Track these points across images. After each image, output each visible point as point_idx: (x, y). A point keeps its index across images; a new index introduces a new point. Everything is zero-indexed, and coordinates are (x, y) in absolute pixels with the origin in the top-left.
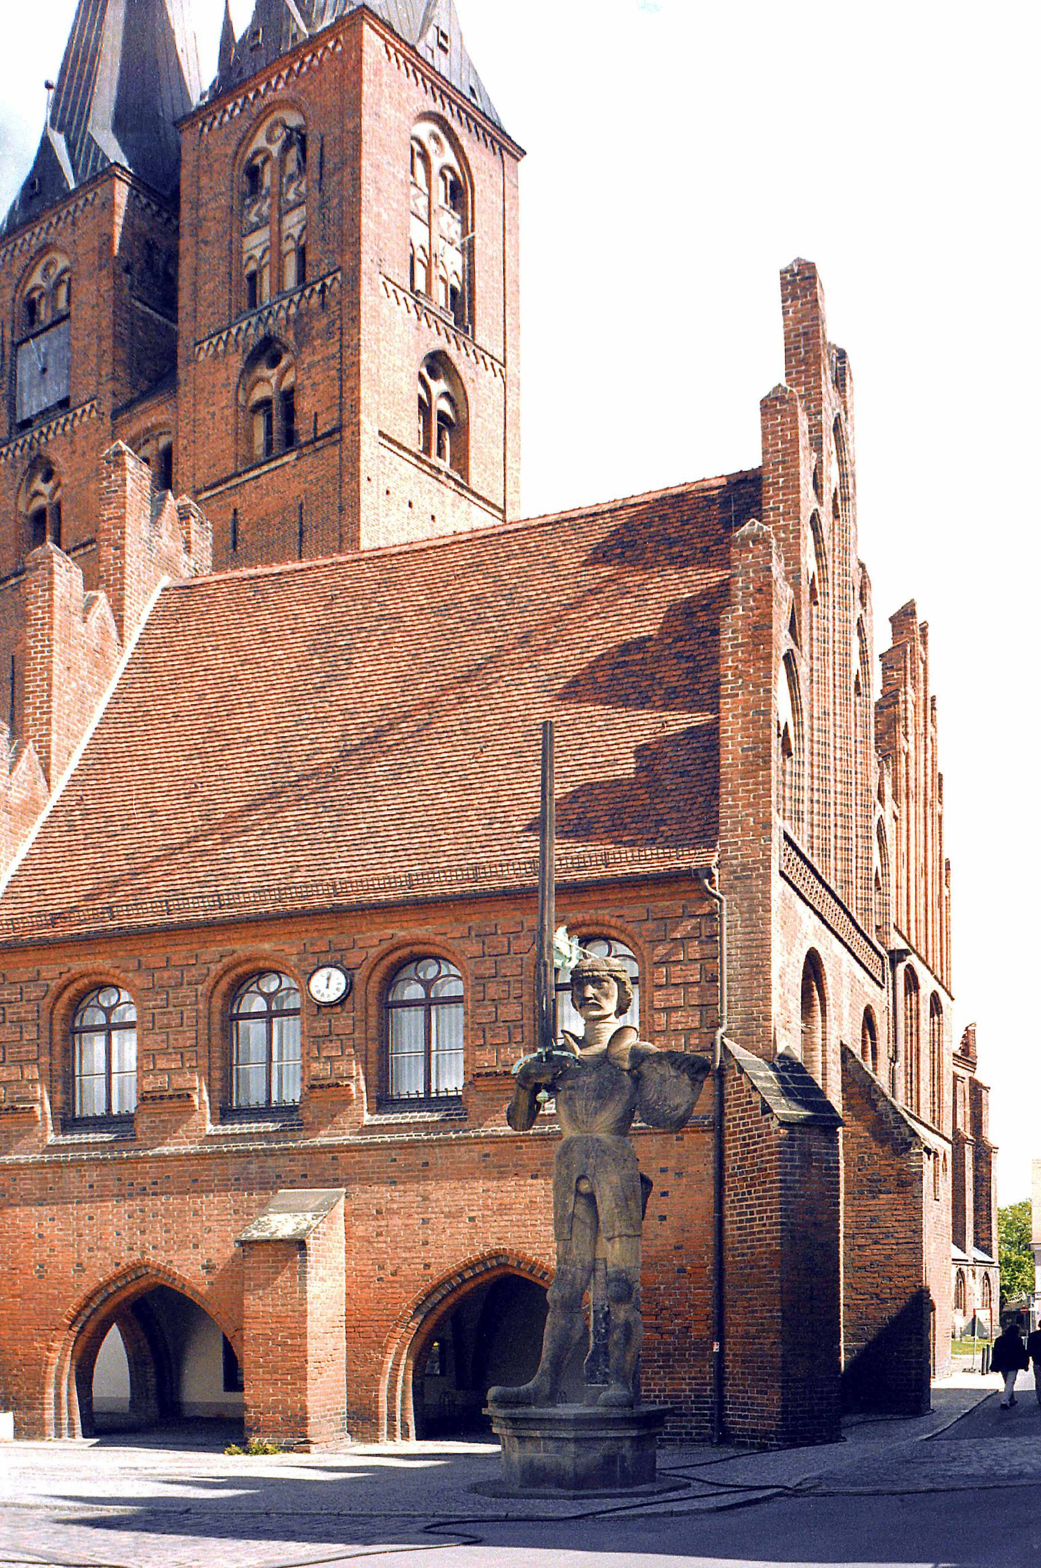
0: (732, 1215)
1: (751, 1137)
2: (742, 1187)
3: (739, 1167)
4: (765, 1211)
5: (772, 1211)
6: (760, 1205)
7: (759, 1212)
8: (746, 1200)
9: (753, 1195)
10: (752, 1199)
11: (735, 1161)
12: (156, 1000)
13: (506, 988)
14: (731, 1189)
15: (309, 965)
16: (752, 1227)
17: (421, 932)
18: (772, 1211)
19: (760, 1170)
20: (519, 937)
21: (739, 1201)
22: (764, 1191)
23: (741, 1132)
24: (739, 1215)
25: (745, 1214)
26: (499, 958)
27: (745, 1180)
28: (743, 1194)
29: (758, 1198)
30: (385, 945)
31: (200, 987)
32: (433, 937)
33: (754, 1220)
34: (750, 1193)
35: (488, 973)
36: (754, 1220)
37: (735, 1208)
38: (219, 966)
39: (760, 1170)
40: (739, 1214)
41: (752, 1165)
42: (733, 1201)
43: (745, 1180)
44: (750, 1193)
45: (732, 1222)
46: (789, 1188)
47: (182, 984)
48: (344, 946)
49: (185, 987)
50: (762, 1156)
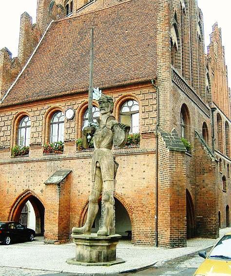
46: (172, 170)
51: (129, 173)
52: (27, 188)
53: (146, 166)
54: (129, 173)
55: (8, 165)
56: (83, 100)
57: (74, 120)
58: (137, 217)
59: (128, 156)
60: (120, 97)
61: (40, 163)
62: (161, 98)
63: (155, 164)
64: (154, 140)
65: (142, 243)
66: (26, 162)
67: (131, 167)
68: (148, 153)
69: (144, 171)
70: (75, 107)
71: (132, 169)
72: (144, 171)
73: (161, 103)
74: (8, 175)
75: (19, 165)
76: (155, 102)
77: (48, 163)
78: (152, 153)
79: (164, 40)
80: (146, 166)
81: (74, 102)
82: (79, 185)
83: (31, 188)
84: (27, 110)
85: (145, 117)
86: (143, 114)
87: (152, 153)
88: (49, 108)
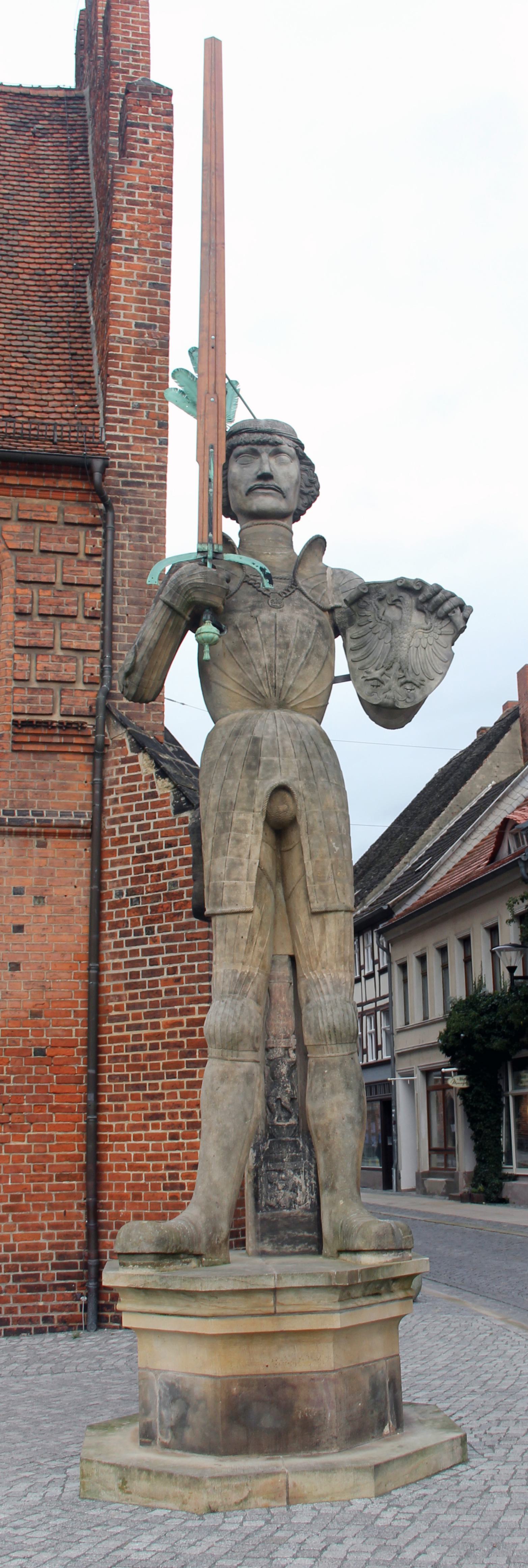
0: (116, 966)
1: (152, 847)
2: (135, 923)
3: (130, 892)
4: (180, 959)
5: (191, 959)
6: (170, 949)
7: (166, 961)
8: (144, 941)
9: (156, 934)
10: (154, 940)
11: (125, 882)
14: (114, 925)
16: (154, 984)
18: (191, 959)
19: (168, 896)
21: (129, 943)
22: (177, 927)
23: (135, 839)
24: (129, 964)
25: (142, 963)
27: (142, 911)
28: (138, 933)
29: (165, 939)
33: (160, 972)
34: (150, 931)
36: (160, 972)
37: (123, 955)
39: (168, 896)
40: (129, 964)
41: (156, 888)
42: (118, 945)
43: (142, 911)
44: (150, 931)
45: (116, 977)
50: (174, 875)
63: (80, 896)
64: (79, 768)
68: (46, 831)
69: (19, 929)
72: (19, 929)
76: (92, 573)
78: (67, 831)
79: (148, 294)
80: (28, 898)
85: (33, 641)
86: (23, 626)
87: (67, 831)
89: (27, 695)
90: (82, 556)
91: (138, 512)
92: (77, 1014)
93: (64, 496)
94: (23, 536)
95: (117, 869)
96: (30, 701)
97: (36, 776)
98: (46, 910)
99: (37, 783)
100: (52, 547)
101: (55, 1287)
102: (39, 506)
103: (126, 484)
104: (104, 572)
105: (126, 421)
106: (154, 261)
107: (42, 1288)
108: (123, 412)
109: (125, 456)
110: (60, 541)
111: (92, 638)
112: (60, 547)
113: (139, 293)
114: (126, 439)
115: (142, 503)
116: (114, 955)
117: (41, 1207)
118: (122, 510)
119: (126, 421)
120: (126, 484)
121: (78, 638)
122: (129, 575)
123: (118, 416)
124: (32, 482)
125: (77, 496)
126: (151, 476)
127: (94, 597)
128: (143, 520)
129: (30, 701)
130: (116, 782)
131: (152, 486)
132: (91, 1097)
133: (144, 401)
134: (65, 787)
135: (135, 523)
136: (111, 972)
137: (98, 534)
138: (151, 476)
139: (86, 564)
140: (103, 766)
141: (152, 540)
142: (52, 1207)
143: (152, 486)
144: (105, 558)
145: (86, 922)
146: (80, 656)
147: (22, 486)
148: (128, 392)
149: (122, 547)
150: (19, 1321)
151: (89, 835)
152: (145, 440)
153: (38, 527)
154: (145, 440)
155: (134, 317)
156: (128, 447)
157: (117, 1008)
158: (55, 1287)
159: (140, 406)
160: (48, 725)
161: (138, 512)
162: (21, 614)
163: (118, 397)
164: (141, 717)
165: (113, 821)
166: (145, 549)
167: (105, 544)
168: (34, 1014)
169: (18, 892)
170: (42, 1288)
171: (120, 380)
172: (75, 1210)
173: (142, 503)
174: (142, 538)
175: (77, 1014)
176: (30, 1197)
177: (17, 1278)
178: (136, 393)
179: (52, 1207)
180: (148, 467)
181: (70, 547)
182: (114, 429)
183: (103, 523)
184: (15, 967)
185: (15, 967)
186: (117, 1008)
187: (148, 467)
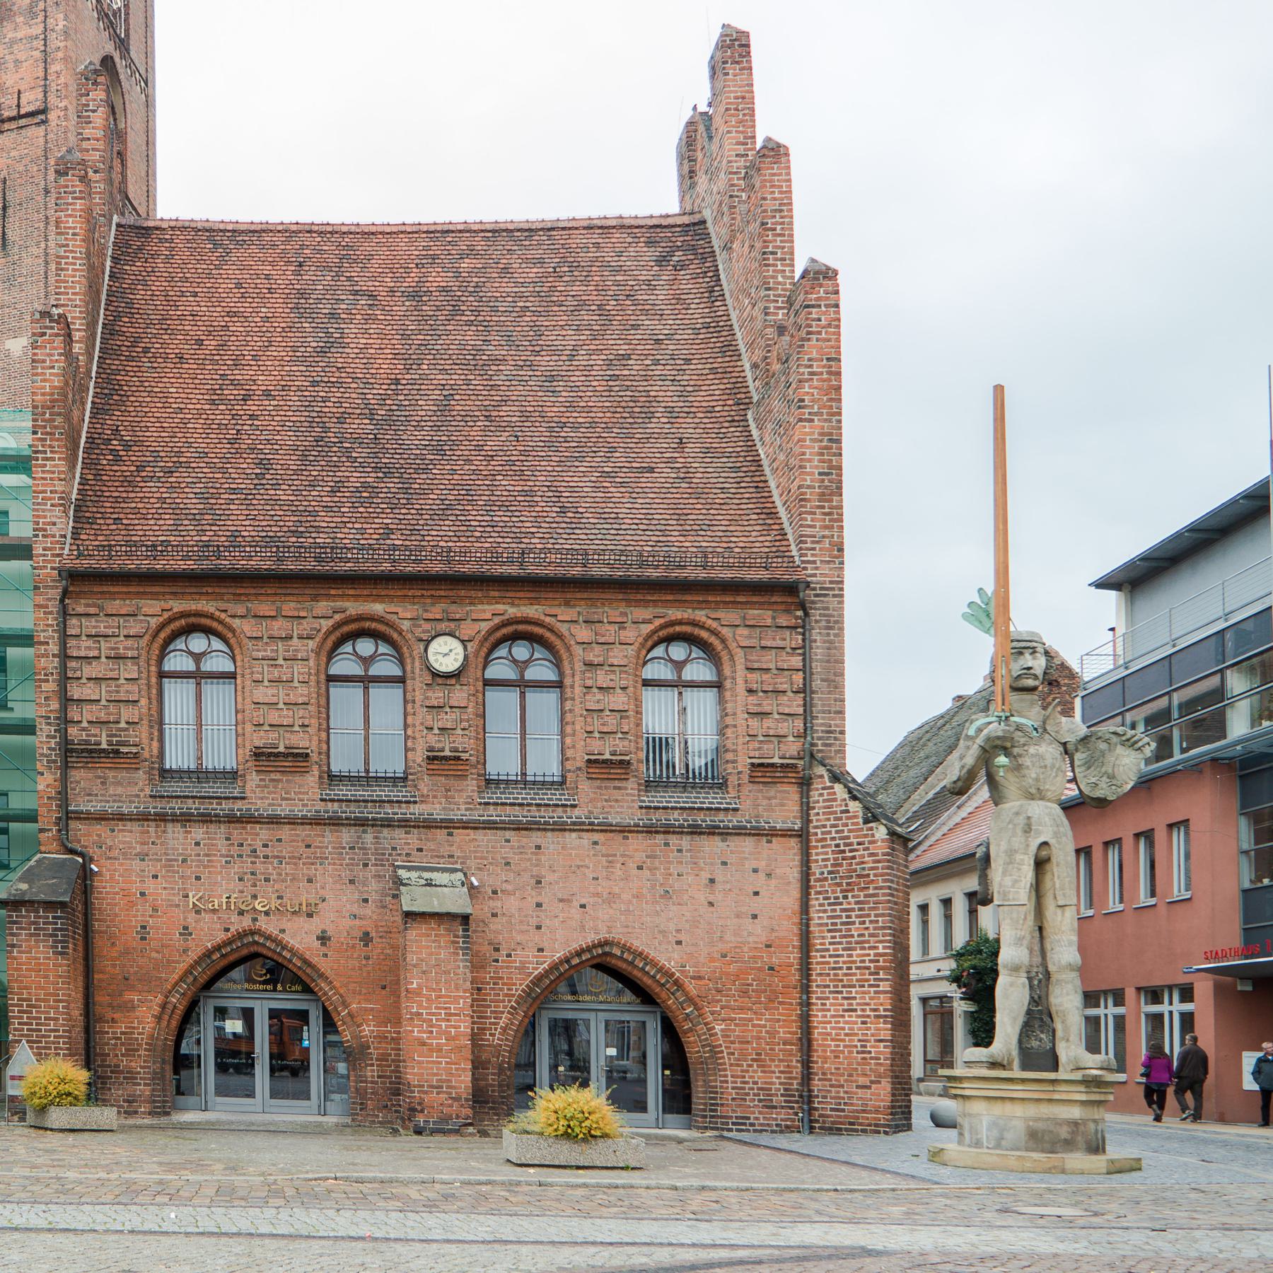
12: (265, 650)
13: (612, 677)
15: (424, 632)
17: (532, 611)
20: (625, 628)
26: (606, 647)
30: (497, 620)
31: (311, 642)
32: (542, 617)
35: (596, 661)
38: (330, 622)
42: (820, 905)
47: (291, 638)
48: (458, 616)
49: (295, 640)
51: (702, 897)
52: (246, 922)
53: (762, 875)
54: (702, 897)
55: (135, 827)
56: (500, 608)
57: (463, 680)
58: (733, 1042)
59: (696, 837)
60: (658, 622)
61: (304, 832)
62: (818, 652)
65: (752, 1125)
66: (232, 819)
67: (705, 875)
69: (756, 893)
70: (468, 629)
71: (712, 881)
72: (756, 893)
73: (817, 667)
74: (136, 864)
75: (198, 832)
76: (796, 661)
77: (347, 835)
78: (786, 834)
80: (762, 875)
81: (458, 611)
82: (496, 925)
83: (269, 926)
84: (223, 605)
88: (338, 617)
89: (757, 745)
90: (788, 650)
91: (825, 615)
92: (794, 947)
93: (775, 607)
94: (750, 637)
95: (820, 857)
96: (759, 749)
97: (765, 798)
98: (773, 882)
99: (765, 802)
100: (769, 644)
101: (783, 1107)
102: (759, 616)
103: (816, 595)
104: (804, 660)
105: (814, 549)
106: (830, 421)
107: (775, 1107)
108: (813, 542)
109: (815, 575)
110: (774, 639)
111: (798, 706)
112: (774, 644)
113: (820, 448)
114: (814, 562)
115: (827, 609)
116: (819, 911)
117: (773, 1061)
118: (815, 614)
119: (814, 549)
120: (816, 595)
121: (789, 706)
122: (821, 661)
123: (808, 545)
124: (755, 599)
125: (783, 607)
126: (833, 589)
127: (798, 678)
128: (828, 622)
129: (759, 749)
130: (818, 802)
131: (834, 596)
132: (805, 997)
133: (827, 533)
134: (783, 805)
135: (824, 623)
136: (817, 921)
137: (800, 633)
138: (833, 589)
139: (792, 655)
140: (809, 791)
141: (836, 635)
142: (780, 1061)
143: (834, 596)
144: (804, 650)
145: (798, 890)
146: (790, 719)
147: (747, 602)
148: (814, 527)
149: (815, 641)
150: (761, 1125)
151: (800, 836)
152: (829, 562)
153: (758, 630)
154: (829, 562)
155: (817, 467)
156: (817, 568)
157: (822, 944)
158: (783, 1107)
159: (824, 537)
160: (772, 765)
161: (825, 615)
162: (750, 691)
163: (808, 531)
164: (831, 758)
165: (816, 827)
166: (831, 642)
167: (804, 640)
168: (768, 946)
169: (755, 871)
170: (775, 1107)
171: (809, 517)
172: (794, 1063)
173: (827, 609)
174: (828, 635)
175: (794, 947)
176: (767, 1055)
177: (760, 1101)
178: (821, 527)
179: (780, 1061)
180: (831, 582)
181: (780, 643)
182: (806, 555)
183: (803, 627)
184: (755, 917)
185: (755, 917)
186: (822, 944)
187: (831, 582)
